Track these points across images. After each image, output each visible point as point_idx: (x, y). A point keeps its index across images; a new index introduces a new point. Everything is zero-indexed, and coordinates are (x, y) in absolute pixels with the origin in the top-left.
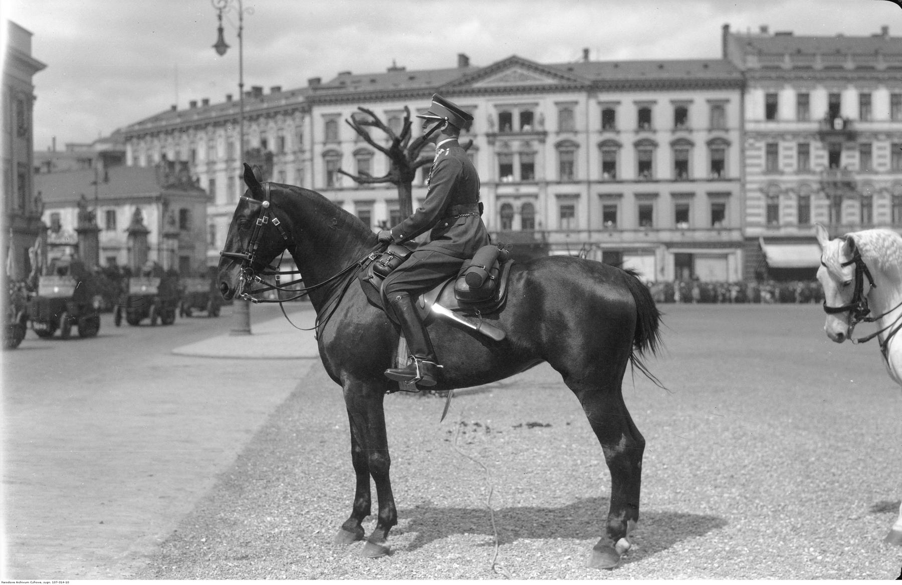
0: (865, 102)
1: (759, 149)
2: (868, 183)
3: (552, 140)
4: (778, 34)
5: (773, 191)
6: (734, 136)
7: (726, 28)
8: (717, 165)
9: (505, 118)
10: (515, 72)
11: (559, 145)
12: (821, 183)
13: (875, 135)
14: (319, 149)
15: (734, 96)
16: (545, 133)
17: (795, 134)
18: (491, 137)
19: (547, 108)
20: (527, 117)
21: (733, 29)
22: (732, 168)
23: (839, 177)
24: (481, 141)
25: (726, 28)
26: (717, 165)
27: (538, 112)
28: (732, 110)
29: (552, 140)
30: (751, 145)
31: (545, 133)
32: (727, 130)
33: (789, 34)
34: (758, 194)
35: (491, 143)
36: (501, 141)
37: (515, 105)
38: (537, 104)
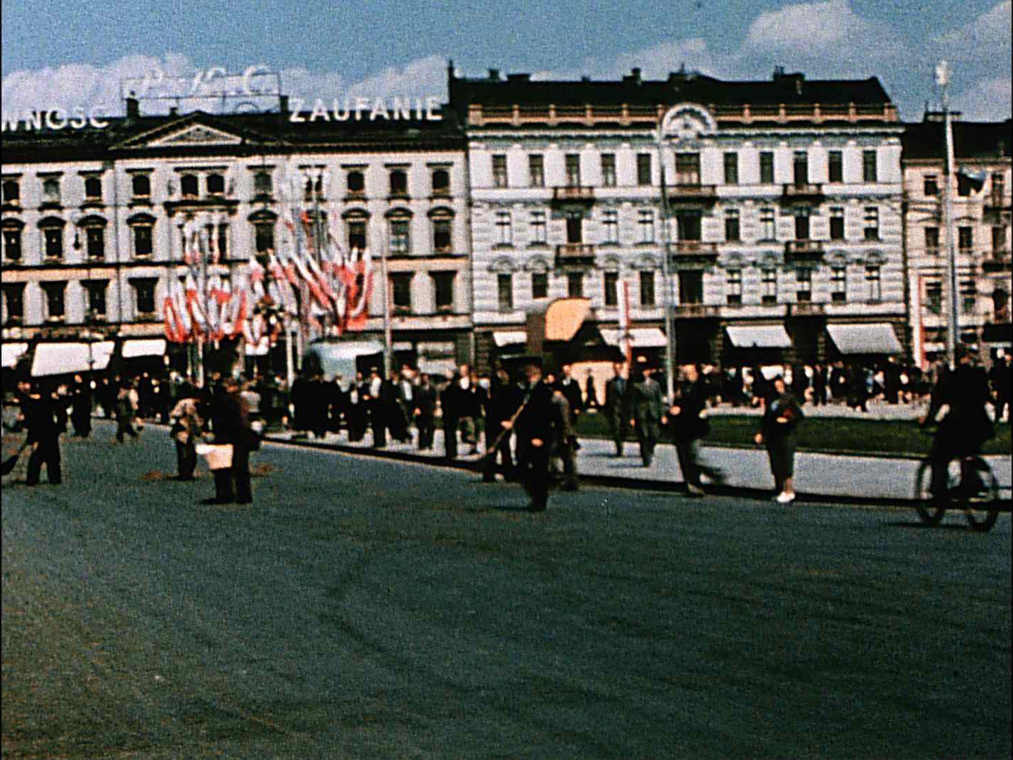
0: (608, 162)
3: (244, 210)
5: (506, 270)
6: (458, 205)
8: (442, 238)
9: (189, 184)
10: (198, 130)
11: (252, 218)
15: (456, 157)
16: (237, 202)
18: (170, 208)
19: (238, 171)
20: (216, 182)
22: (458, 246)
23: (577, 253)
24: (158, 211)
26: (442, 238)
27: (227, 176)
28: (455, 175)
29: (244, 210)
30: (478, 215)
31: (237, 202)
32: (450, 198)
34: (486, 273)
35: (170, 214)
36: (183, 211)
37: (202, 169)
38: (225, 168)
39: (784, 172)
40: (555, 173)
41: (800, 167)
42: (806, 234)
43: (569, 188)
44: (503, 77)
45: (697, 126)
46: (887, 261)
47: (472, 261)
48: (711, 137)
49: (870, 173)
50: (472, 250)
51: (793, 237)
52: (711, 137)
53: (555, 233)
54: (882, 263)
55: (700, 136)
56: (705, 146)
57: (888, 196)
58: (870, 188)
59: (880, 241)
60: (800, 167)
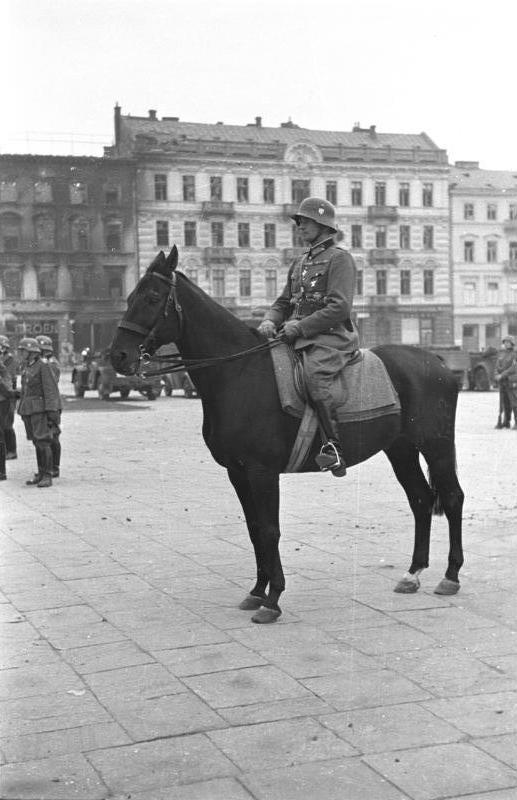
1: (150, 227)
2: (247, 260)
4: (164, 119)
7: (118, 109)
12: (205, 259)
13: (252, 215)
17: (182, 214)
21: (124, 113)
23: (221, 255)
25: (118, 109)
30: (144, 222)
33: (176, 119)
39: (369, 198)
40: (203, 191)
41: (380, 192)
44: (159, 116)
45: (309, 159)
46: (440, 266)
47: (138, 259)
48: (319, 167)
49: (428, 199)
50: (138, 250)
51: (374, 247)
52: (319, 167)
53: (205, 239)
54: (436, 267)
55: (311, 168)
56: (315, 175)
57: (441, 218)
58: (430, 212)
59: (435, 251)
60: (380, 192)
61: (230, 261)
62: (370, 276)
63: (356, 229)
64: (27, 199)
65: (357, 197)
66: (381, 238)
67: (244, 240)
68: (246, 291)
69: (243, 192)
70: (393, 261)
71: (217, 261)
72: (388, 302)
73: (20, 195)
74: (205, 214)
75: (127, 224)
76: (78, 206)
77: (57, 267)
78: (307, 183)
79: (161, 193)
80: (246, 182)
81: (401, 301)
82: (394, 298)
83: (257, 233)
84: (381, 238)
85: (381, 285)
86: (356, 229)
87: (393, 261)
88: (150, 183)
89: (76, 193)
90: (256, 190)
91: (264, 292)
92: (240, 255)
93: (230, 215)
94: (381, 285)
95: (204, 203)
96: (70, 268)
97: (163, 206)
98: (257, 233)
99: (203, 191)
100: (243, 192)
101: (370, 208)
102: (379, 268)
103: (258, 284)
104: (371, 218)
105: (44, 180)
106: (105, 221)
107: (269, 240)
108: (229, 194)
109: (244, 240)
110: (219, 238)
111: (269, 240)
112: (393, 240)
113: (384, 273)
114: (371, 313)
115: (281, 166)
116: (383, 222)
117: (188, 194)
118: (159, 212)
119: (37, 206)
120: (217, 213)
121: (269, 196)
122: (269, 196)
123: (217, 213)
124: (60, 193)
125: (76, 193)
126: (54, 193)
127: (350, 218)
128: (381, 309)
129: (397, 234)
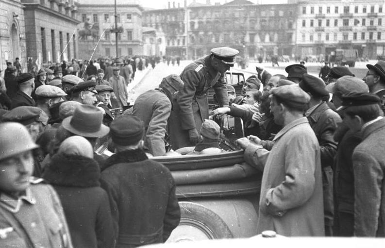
14: (189, 21)
42: (373, 24)
43: (319, 14)
55: (350, 2)
61: (323, 30)
62: (375, 34)
63: (364, 20)
64: (268, 16)
65: (365, 10)
66: (372, 22)
67: (328, 24)
68: (327, 38)
69: (328, 11)
70: (375, 29)
71: (319, 30)
72: (372, 42)
73: (266, 14)
74: (316, 18)
75: (294, 21)
76: (281, 17)
77: (274, 34)
78: (348, 7)
79: (304, 12)
80: (329, 8)
81: (377, 41)
82: (375, 40)
83: (332, 22)
84: (372, 22)
85: (371, 37)
86: (364, 20)
87: (375, 29)
88: (301, 9)
89: (281, 13)
90: (332, 10)
91: (333, 39)
92: (326, 28)
93: (324, 17)
94: (371, 37)
95: (316, 15)
96: (278, 33)
97: (304, 16)
98: (332, 22)
99: (316, 11)
100: (328, 11)
101: (369, 14)
102: (371, 31)
103: (331, 37)
104: (369, 17)
105: (272, 10)
106: (288, 20)
107: (336, 24)
108: (324, 11)
109: (328, 24)
110: (320, 24)
111: (336, 24)
112: (376, 23)
113: (372, 33)
114: (367, 45)
115: (341, 3)
116: (373, 18)
117: (312, 12)
118: (303, 18)
119: (270, 17)
120: (320, 17)
121: (336, 11)
122: (336, 11)
123: (320, 17)
124: (277, 13)
125: (281, 13)
126: (275, 13)
127: (361, 17)
128: (370, 44)
129: (377, 21)
